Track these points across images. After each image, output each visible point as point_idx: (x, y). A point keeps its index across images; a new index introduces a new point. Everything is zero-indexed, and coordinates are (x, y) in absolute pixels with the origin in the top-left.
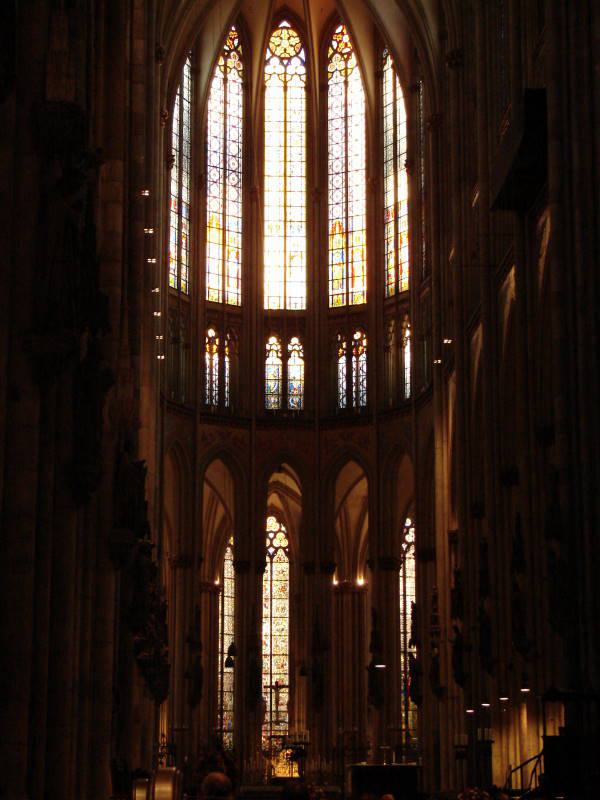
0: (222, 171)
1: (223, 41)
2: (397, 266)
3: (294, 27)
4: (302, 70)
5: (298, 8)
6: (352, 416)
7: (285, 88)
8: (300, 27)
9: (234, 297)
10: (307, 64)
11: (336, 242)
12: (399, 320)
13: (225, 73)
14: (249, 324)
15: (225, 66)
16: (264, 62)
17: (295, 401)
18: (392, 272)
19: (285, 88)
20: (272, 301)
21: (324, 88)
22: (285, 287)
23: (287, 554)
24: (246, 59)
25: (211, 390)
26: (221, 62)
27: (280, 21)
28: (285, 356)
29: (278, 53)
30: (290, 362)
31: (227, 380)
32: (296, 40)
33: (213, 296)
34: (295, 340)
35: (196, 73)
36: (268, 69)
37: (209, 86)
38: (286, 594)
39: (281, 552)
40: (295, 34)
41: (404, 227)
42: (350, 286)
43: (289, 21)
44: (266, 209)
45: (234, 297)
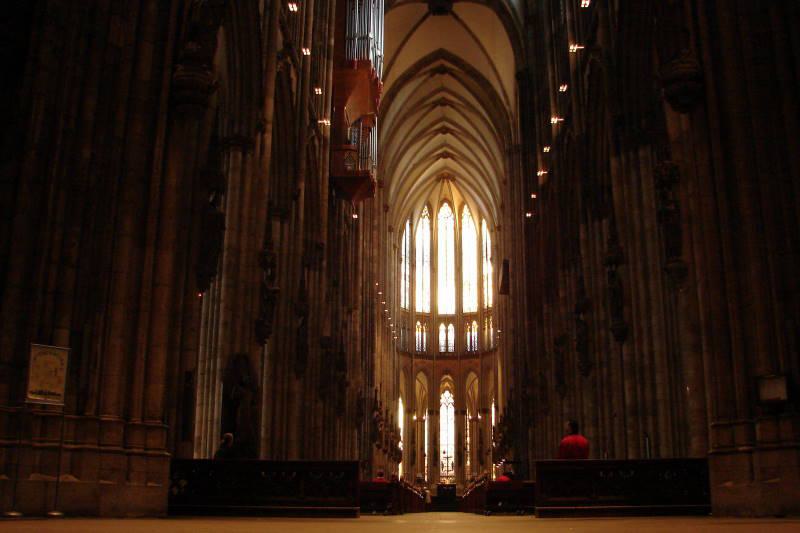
5: (449, 198)
6: (471, 355)
8: (451, 205)
9: (427, 310)
12: (489, 318)
17: (451, 349)
21: (460, 229)
28: (447, 331)
32: (450, 210)
35: (411, 225)
42: (470, 306)
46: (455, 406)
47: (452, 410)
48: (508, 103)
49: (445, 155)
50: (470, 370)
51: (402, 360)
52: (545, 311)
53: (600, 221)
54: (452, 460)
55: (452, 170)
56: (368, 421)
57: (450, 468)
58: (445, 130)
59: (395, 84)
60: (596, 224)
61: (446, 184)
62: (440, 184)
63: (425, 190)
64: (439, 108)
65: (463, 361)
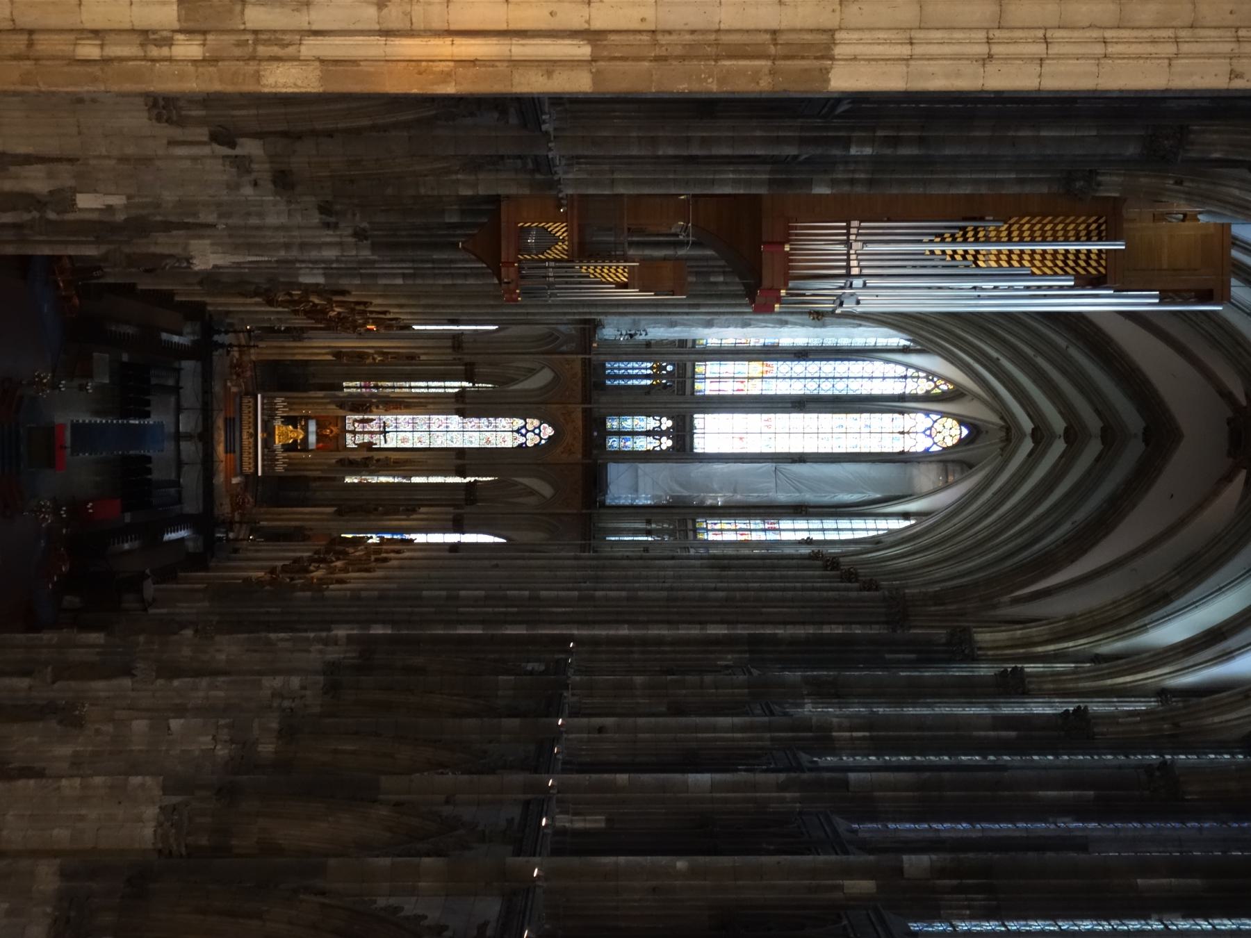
0: (817, 375)
2: (722, 530)
3: (961, 441)
4: (920, 449)
7: (903, 433)
12: (671, 533)
13: (912, 377)
14: (679, 400)
15: (918, 377)
16: (927, 413)
18: (718, 527)
19: (903, 433)
20: (700, 420)
22: (714, 434)
23: (520, 446)
24: (928, 397)
25: (619, 369)
27: (966, 427)
30: (650, 439)
31: (630, 383)
32: (950, 442)
34: (670, 443)
36: (921, 416)
38: (483, 445)
39: (522, 440)
40: (955, 441)
41: (755, 536)
43: (967, 436)
44: (786, 416)
45: (705, 388)
54: (379, 441)
57: (360, 439)
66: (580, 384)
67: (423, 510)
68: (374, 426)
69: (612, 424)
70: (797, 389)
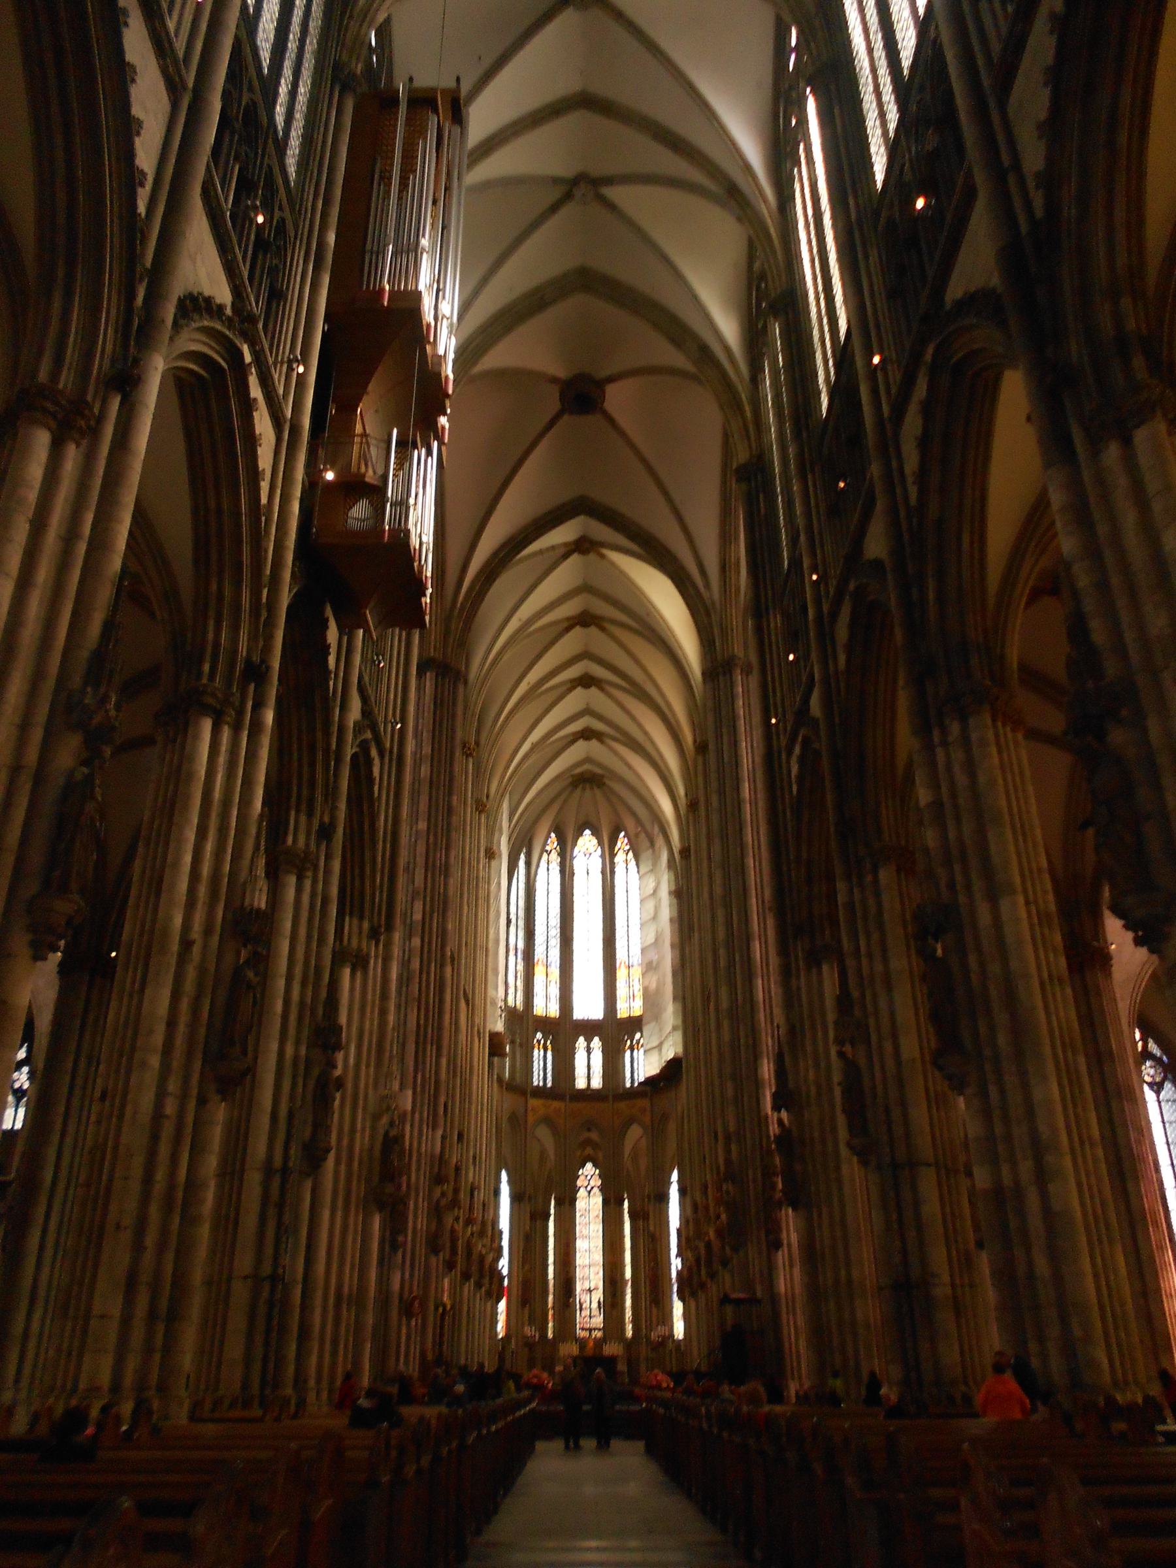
1: (545, 844)
4: (600, 860)
8: (596, 833)
9: (554, 1011)
10: (603, 856)
11: (621, 974)
14: (564, 1031)
16: (572, 858)
17: (597, 1083)
21: (613, 872)
22: (588, 1005)
26: (545, 855)
28: (589, 1050)
29: (583, 850)
32: (595, 841)
33: (539, 1009)
34: (596, 1039)
35: (528, 864)
36: (575, 862)
37: (536, 874)
39: (596, 1190)
45: (554, 1011)
46: (603, 1189)
47: (597, 1200)
48: (707, 585)
49: (587, 734)
50: (631, 1121)
51: (510, 1102)
52: (841, 898)
53: (1127, 441)
54: (598, 1295)
55: (600, 765)
56: (423, 1205)
57: (595, 1312)
58: (586, 681)
59: (495, 554)
60: (1112, 453)
61: (588, 793)
62: (579, 790)
63: (552, 801)
64: (578, 629)
65: (622, 1105)
66: (550, 1102)
67: (652, 1228)
68: (585, 1298)
69: (581, 1084)
70: (555, 943)
